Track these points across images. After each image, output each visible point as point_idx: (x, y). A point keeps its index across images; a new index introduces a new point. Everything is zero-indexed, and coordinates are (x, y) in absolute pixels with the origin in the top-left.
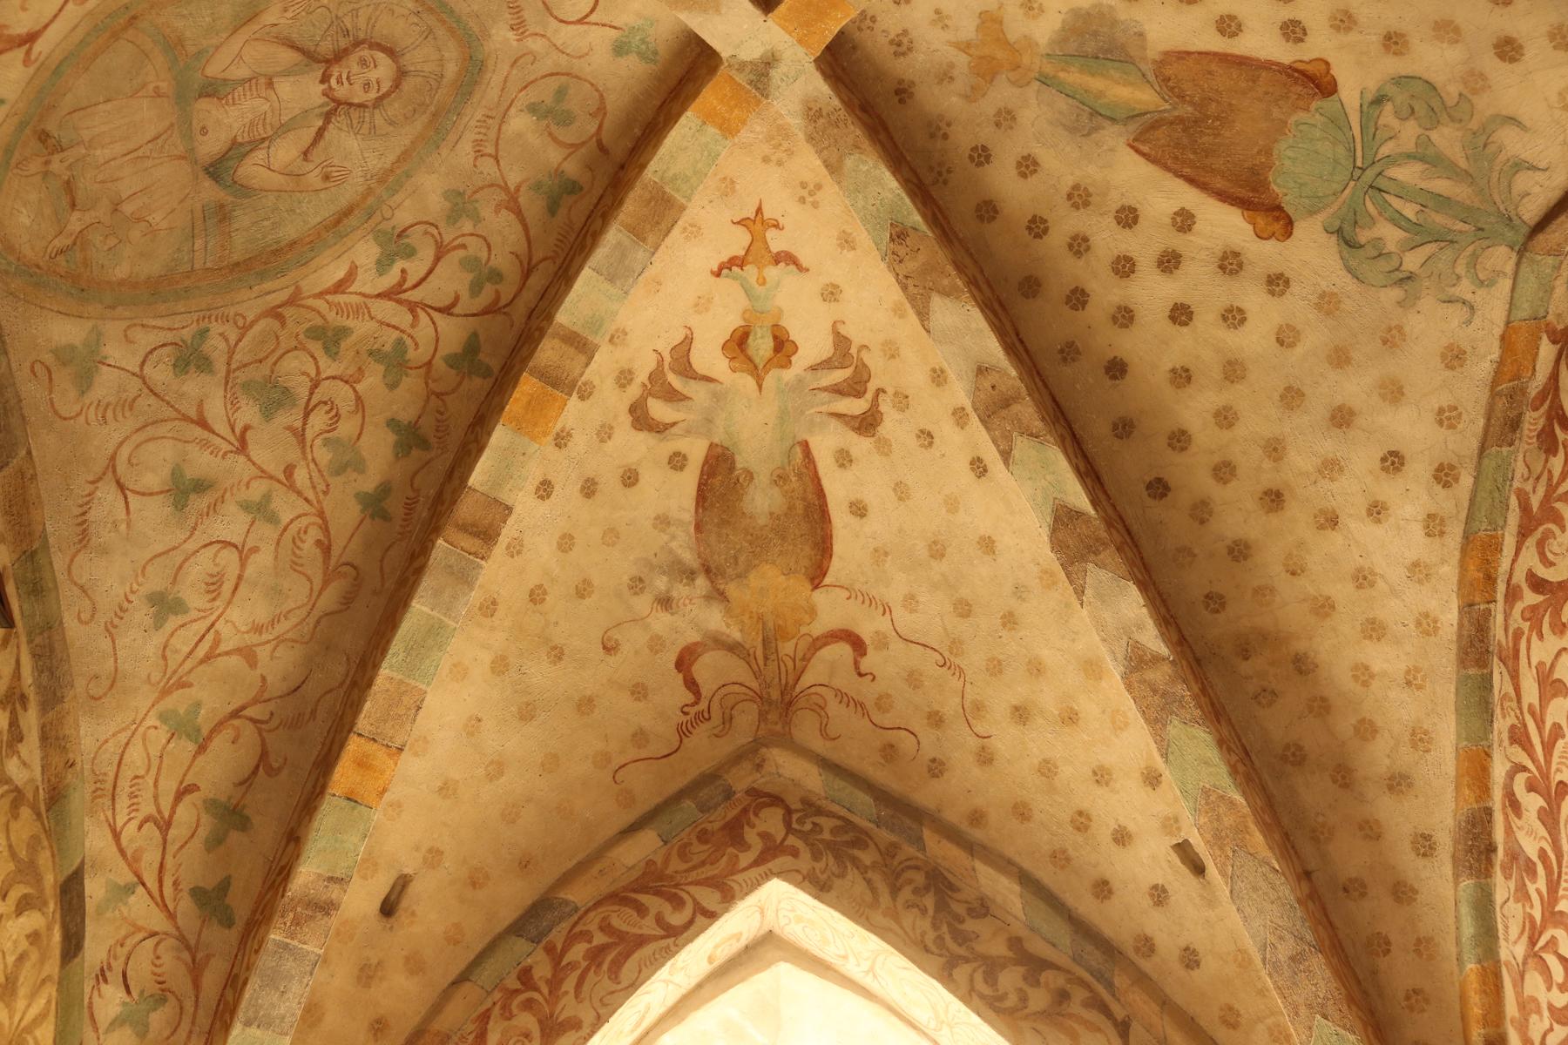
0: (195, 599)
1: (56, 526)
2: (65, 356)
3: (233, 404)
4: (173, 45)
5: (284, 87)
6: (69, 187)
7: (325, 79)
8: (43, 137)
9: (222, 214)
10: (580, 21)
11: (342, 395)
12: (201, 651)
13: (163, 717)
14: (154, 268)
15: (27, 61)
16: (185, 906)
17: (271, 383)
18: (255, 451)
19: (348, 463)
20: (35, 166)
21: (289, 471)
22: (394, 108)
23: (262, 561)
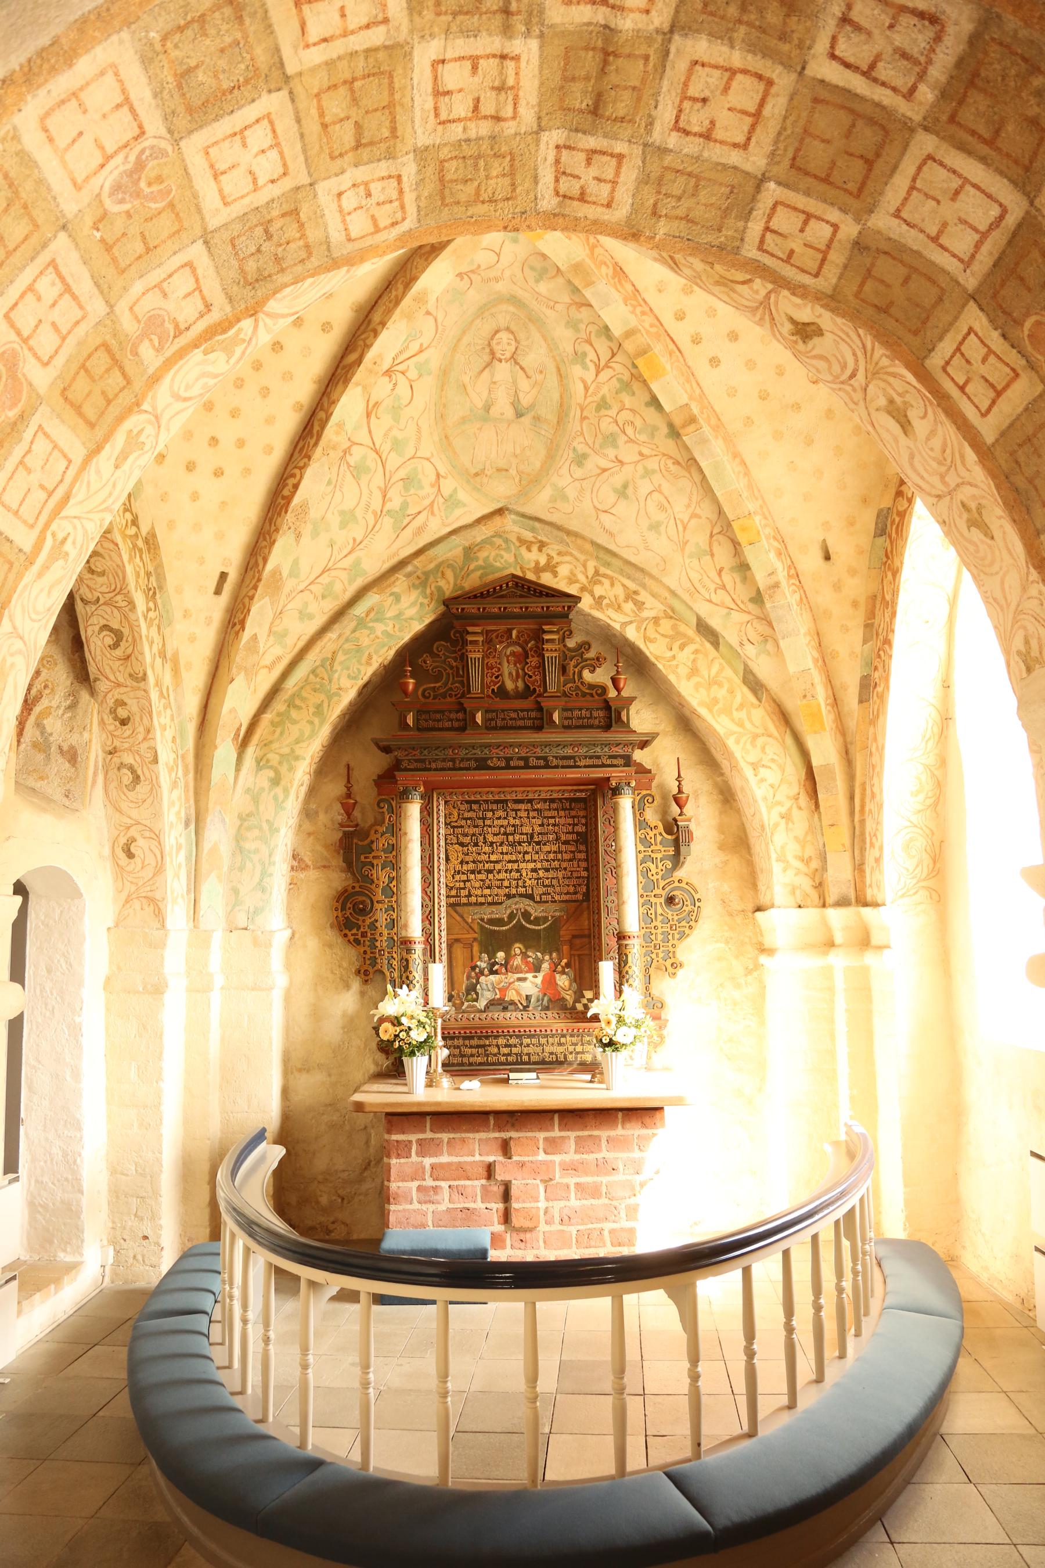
0: (661, 517)
1: (602, 540)
2: (553, 499)
3: (605, 456)
4: (464, 420)
5: (497, 377)
6: (499, 470)
7: (500, 361)
8: (477, 474)
9: (537, 419)
10: (498, 255)
11: (625, 415)
12: (680, 528)
13: (691, 556)
14: (543, 453)
15: (445, 478)
16: (751, 607)
17: (606, 438)
18: (625, 460)
19: (653, 431)
20: (485, 480)
21: (641, 454)
22: (521, 336)
23: (666, 487)
